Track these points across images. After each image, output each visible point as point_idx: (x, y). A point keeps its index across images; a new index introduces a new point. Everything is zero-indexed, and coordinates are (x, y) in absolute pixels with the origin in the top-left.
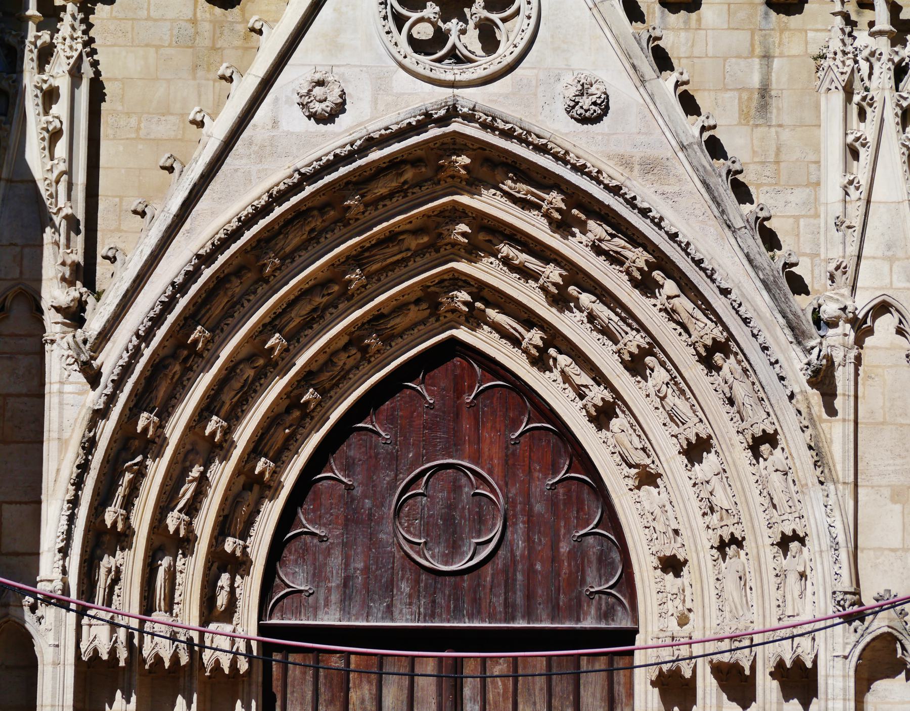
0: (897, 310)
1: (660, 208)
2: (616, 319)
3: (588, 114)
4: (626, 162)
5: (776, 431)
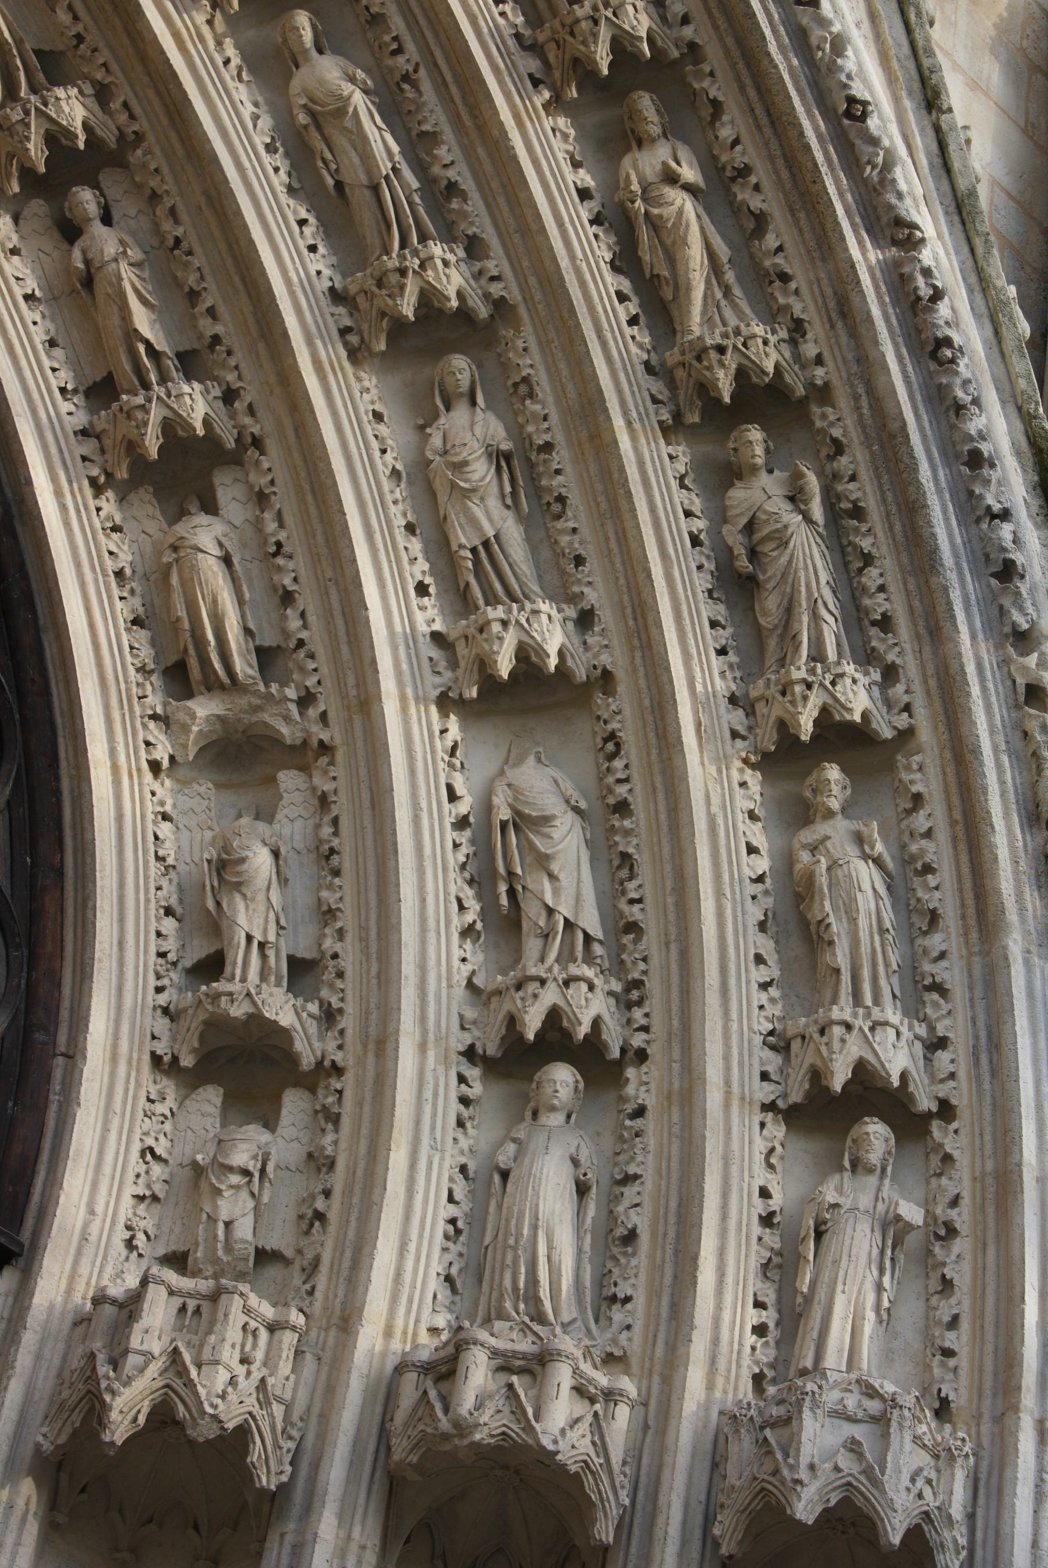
5: (906, 735)
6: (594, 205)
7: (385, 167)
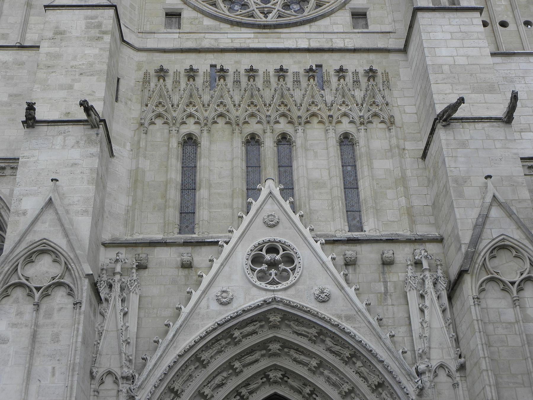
0: (447, 367)
1: (354, 331)
2: (338, 379)
3: (324, 299)
4: (340, 317)
6: (355, 372)
7: (335, 380)
